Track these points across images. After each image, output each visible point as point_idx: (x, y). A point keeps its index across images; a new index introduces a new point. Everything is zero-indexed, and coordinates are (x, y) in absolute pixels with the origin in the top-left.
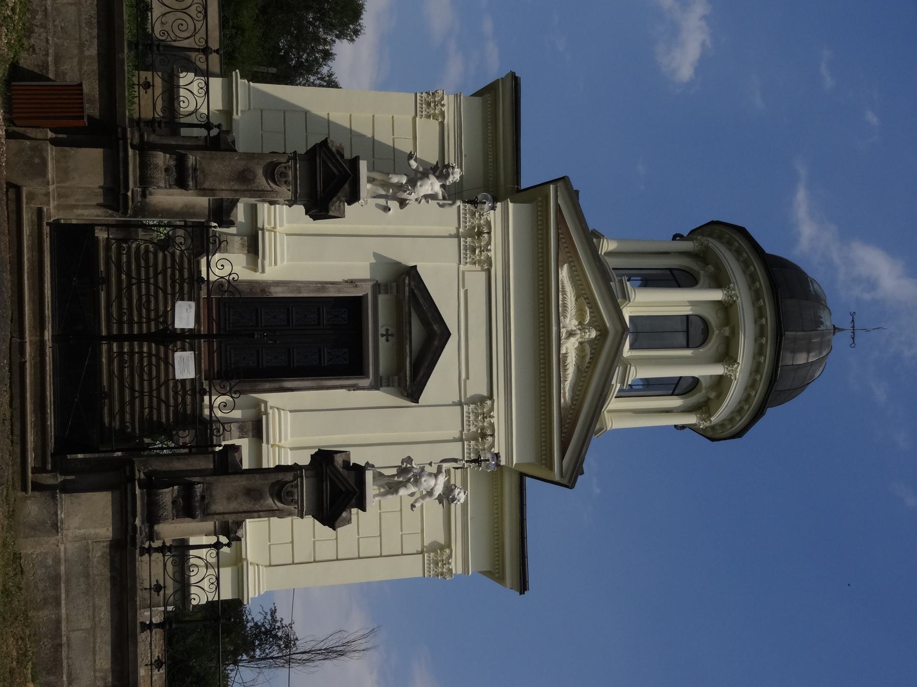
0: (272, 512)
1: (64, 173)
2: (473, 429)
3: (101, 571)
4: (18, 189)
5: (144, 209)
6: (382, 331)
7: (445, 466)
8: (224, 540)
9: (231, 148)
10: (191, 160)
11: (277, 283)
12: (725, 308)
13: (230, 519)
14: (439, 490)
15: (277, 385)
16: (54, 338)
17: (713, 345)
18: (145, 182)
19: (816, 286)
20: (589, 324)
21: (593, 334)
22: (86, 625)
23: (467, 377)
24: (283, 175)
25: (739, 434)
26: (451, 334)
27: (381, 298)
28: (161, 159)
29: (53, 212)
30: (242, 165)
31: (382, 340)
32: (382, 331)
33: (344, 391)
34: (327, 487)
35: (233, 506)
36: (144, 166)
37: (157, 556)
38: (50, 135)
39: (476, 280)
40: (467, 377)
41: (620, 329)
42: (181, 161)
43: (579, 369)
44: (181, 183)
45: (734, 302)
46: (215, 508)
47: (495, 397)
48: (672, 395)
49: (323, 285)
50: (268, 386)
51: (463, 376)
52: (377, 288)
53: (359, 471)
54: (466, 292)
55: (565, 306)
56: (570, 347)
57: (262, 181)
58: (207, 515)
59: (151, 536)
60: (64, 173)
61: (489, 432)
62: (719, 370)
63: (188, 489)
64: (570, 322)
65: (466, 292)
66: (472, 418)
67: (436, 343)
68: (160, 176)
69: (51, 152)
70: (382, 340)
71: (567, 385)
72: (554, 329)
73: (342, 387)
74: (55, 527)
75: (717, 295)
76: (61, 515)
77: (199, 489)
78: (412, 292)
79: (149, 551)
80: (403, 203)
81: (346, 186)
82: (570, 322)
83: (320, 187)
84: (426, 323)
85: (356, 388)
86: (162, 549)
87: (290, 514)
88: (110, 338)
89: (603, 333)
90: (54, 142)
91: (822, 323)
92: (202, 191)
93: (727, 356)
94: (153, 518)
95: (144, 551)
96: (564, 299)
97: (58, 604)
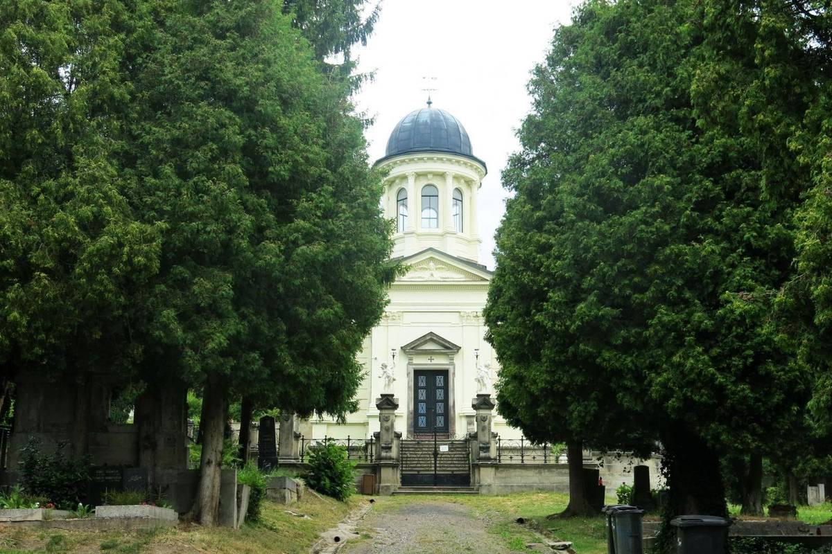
0: (490, 424)
1: (388, 481)
3: (504, 474)
4: (393, 493)
5: (398, 460)
6: (429, 362)
7: (478, 367)
8: (498, 438)
9: (379, 433)
10: (383, 445)
11: (408, 408)
13: (491, 436)
14: (486, 370)
15: (452, 409)
16: (435, 486)
17: (436, 182)
18: (391, 458)
19: (407, 121)
21: (432, 264)
22: (519, 478)
24: (387, 417)
25: (483, 164)
26: (431, 332)
27: (414, 362)
28: (384, 454)
29: (399, 485)
30: (384, 430)
31: (433, 362)
32: (429, 362)
33: (455, 379)
34: (482, 406)
35: (487, 435)
36: (386, 458)
37: (502, 458)
38: (377, 484)
39: (408, 318)
41: (430, 252)
42: (383, 448)
44: (390, 448)
46: (487, 440)
48: (462, 201)
49: (409, 387)
50: (452, 412)
51: (450, 325)
53: (478, 395)
55: (419, 277)
57: (388, 424)
58: (489, 443)
59: (495, 459)
60: (388, 481)
61: (475, 314)
62: (450, 180)
63: (481, 449)
67: (435, 338)
68: (388, 454)
69: (382, 485)
70: (433, 362)
73: (453, 380)
74: (490, 485)
75: (411, 180)
76: (486, 484)
77: (481, 445)
78: (412, 349)
79: (500, 460)
80: (394, 380)
81: (390, 398)
83: (390, 407)
84: (426, 342)
85: (454, 374)
86: (500, 456)
87: (490, 418)
88: (435, 470)
89: (432, 259)
90: (380, 483)
91: (426, 121)
92: (392, 442)
93: (442, 176)
94: (489, 459)
95: (500, 462)
96: (416, 278)
97: (512, 486)
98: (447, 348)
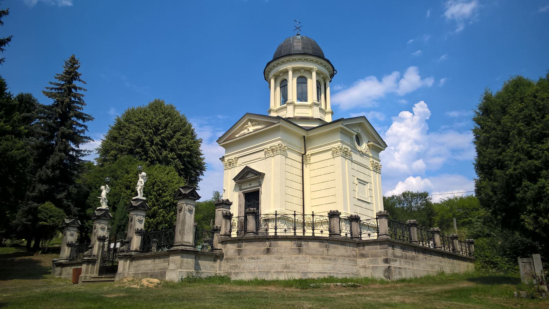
2: (272, 153)
12: (295, 70)
20: (248, 125)
23: (260, 158)
31: (252, 186)
32: (250, 187)
40: (260, 158)
43: (259, 125)
45: (273, 75)
47: (263, 149)
52: (240, 190)
54: (243, 163)
56: (251, 129)
64: (246, 131)
65: (243, 163)
66: (269, 154)
70: (252, 186)
71: (260, 127)
72: (247, 135)
82: (246, 131)
98: (256, 175)
